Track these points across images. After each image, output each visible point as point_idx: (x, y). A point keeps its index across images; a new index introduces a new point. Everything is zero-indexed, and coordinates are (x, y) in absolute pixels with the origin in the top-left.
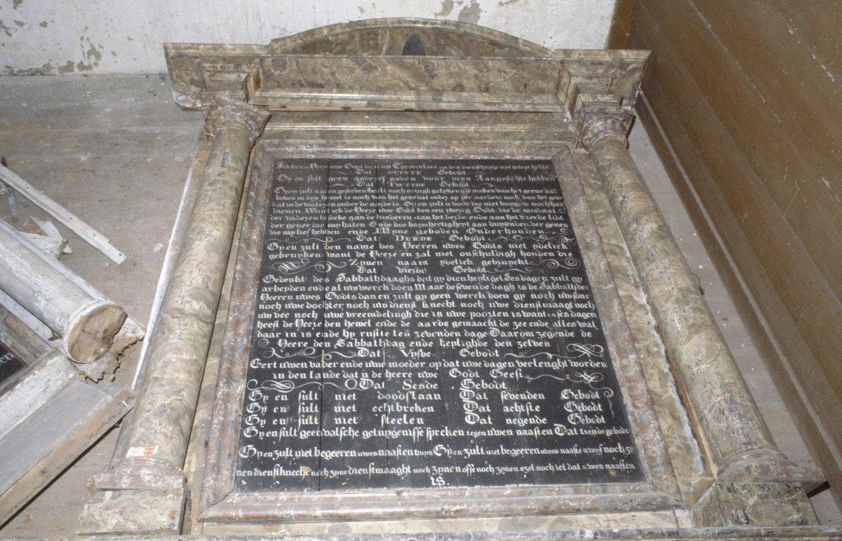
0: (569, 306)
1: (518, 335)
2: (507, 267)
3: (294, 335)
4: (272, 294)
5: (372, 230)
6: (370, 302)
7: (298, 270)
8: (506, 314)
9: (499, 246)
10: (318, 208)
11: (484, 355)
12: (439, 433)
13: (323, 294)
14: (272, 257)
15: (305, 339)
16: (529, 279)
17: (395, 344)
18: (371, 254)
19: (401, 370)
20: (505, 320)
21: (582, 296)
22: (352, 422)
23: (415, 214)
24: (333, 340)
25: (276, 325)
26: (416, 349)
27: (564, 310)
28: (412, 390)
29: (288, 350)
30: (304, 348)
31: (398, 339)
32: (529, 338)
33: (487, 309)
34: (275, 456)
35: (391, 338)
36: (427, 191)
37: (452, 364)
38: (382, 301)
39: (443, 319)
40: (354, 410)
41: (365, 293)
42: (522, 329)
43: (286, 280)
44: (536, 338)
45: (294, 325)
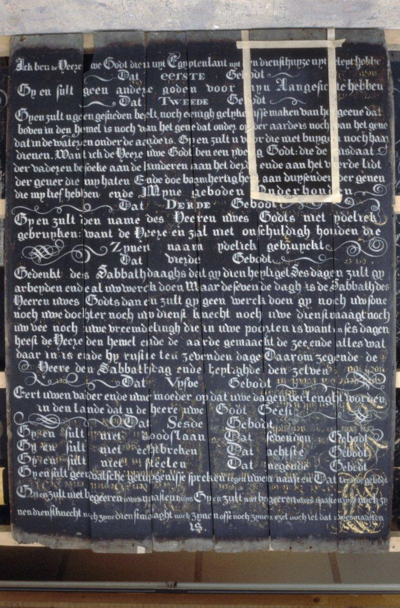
0: (360, 316)
1: (296, 358)
2: (294, 255)
3: (54, 355)
4: (27, 295)
5: (137, 190)
6: (135, 310)
7: (53, 258)
8: (285, 329)
9: (292, 219)
10: (72, 150)
11: (254, 385)
12: (200, 479)
13: (82, 296)
14: (22, 237)
15: (66, 362)
16: (320, 274)
17: (161, 370)
18: (137, 233)
19: (166, 404)
20: (283, 336)
21: (379, 301)
22: (117, 465)
23: (193, 160)
24: (96, 364)
25: (35, 342)
26: (183, 376)
27: (353, 323)
28: (177, 428)
29: (50, 375)
30: (66, 374)
31: (165, 363)
32: (305, 363)
33: (265, 321)
34: (50, 497)
35: (158, 362)
36: (209, 115)
37: (219, 398)
38: (150, 308)
39: (216, 335)
40: (119, 452)
41: (130, 296)
42: (302, 350)
43: (39, 275)
44: (314, 364)
45: (53, 342)
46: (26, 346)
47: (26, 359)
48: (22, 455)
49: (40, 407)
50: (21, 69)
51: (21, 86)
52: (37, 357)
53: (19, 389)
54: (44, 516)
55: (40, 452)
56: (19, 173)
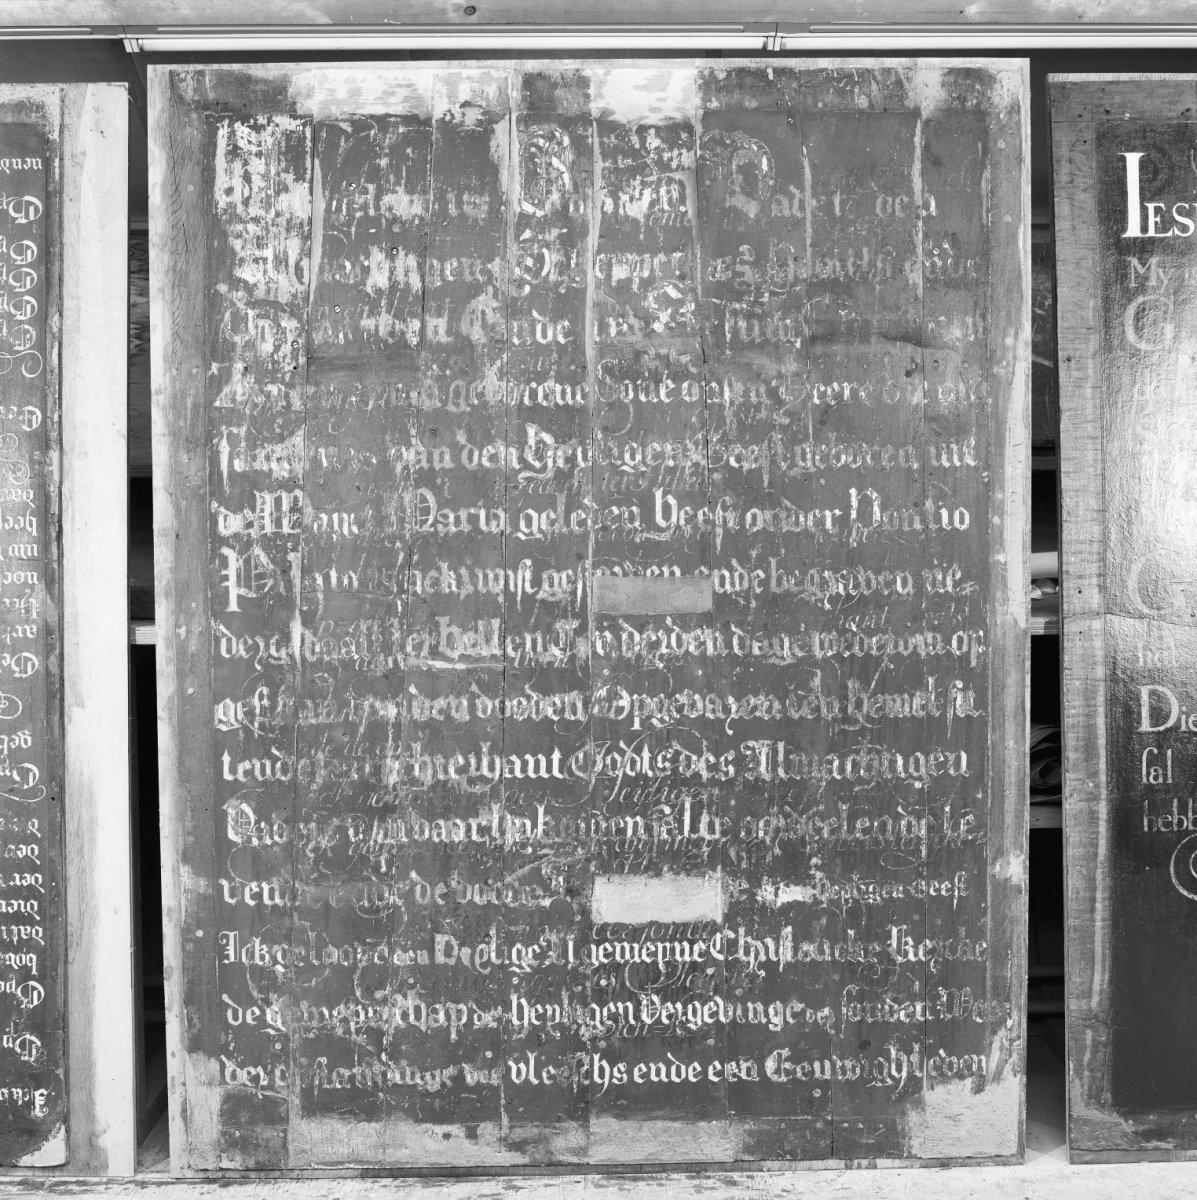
50: (37, 1093)
53: (30, 425)
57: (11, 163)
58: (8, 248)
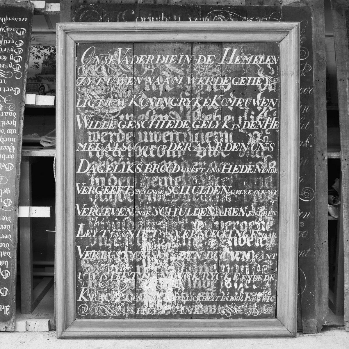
34: (5, 29)
46: (9, 120)
47: (10, 112)
48: (20, 53)
49: (5, 82)
50: (6, 307)
51: (6, 294)
52: (3, 113)
53: (16, 93)
54: (11, 18)
55: (7, 54)
56: (8, 234)
57: (18, 19)
58: (15, 42)
